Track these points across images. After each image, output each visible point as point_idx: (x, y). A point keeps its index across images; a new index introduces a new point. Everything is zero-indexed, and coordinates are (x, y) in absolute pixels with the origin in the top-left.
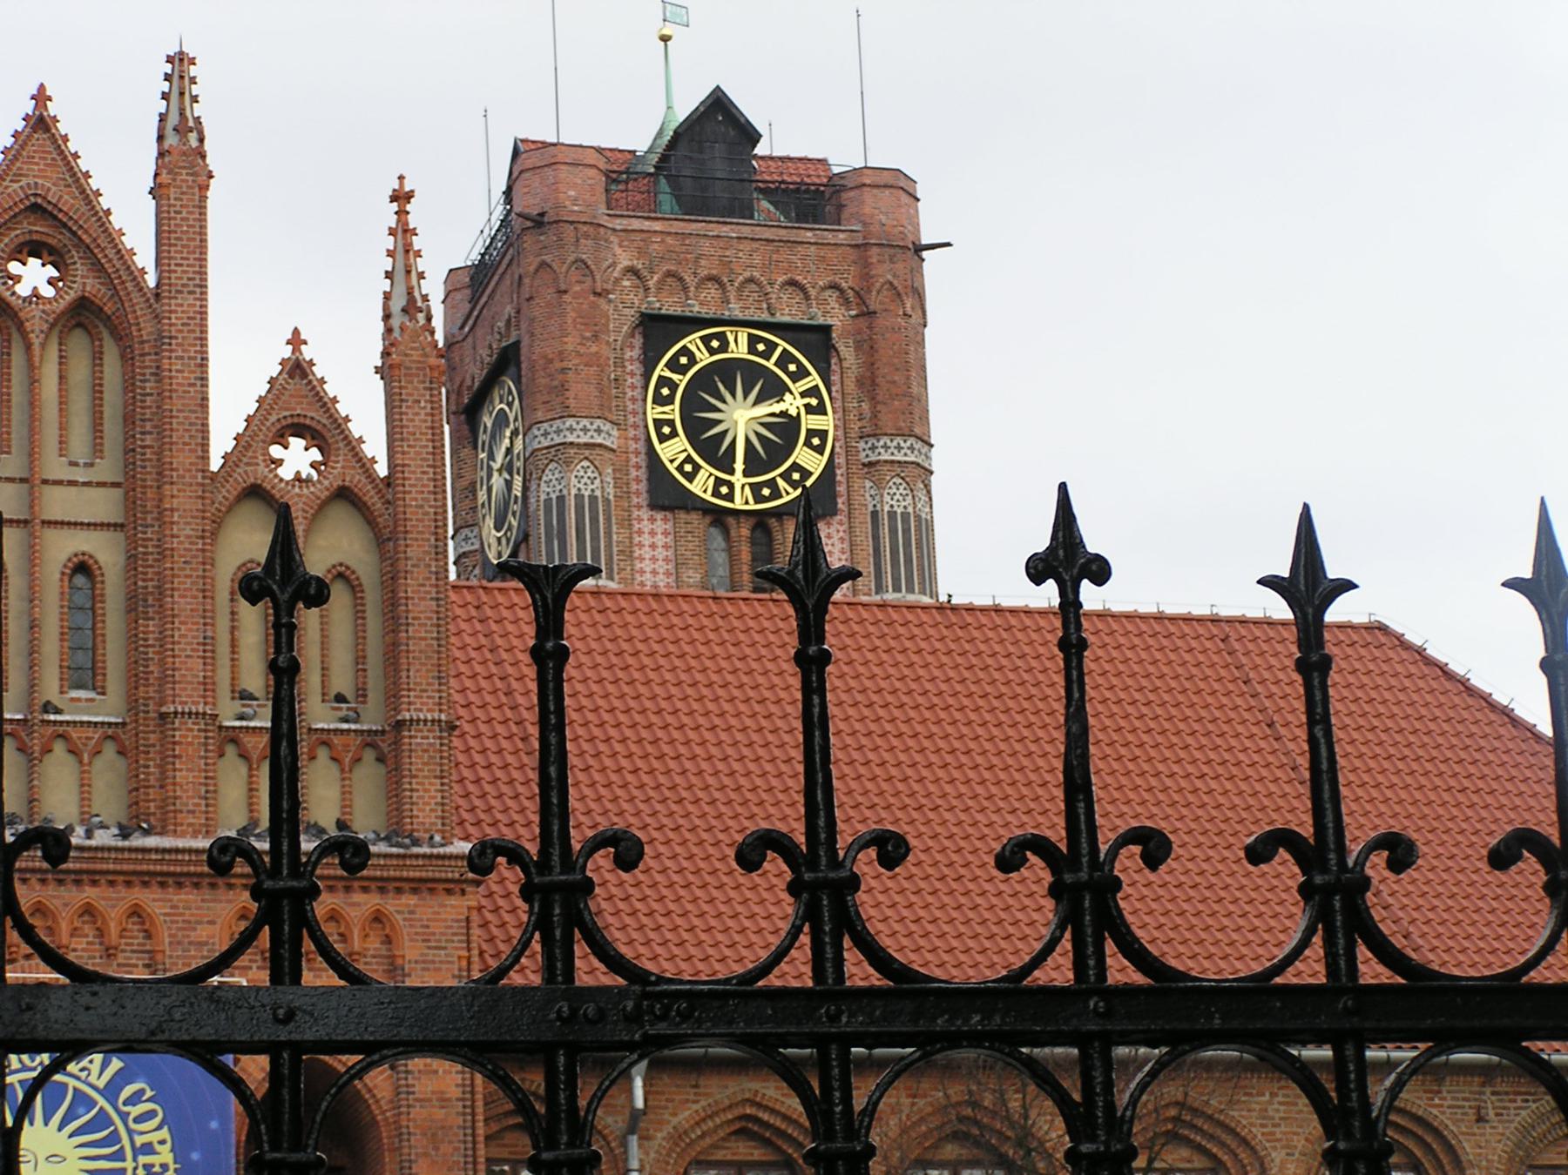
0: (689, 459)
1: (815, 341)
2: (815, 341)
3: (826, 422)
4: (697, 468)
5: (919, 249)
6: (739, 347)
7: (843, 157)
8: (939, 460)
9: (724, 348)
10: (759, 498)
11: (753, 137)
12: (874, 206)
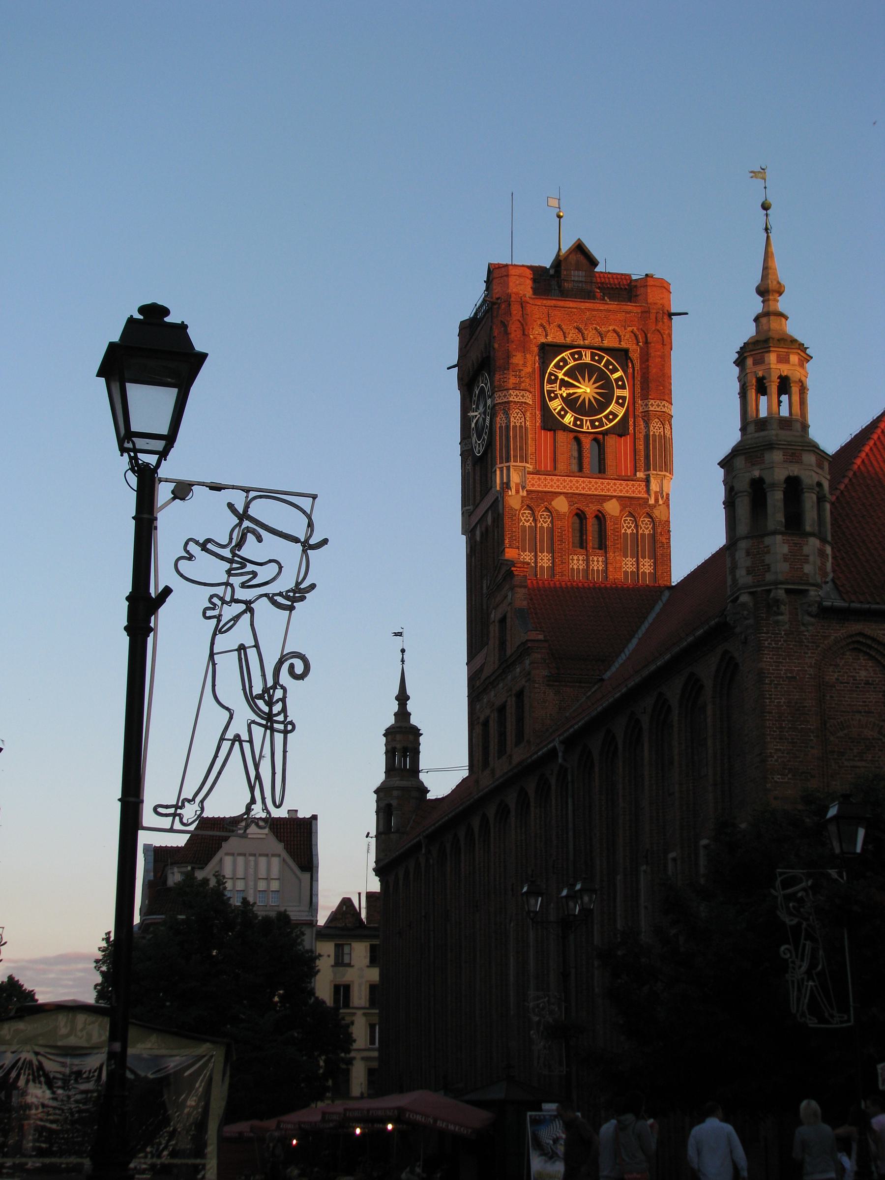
0: (563, 409)
1: (621, 355)
2: (621, 355)
3: (626, 393)
4: (566, 413)
5: (670, 315)
6: (587, 359)
7: (637, 273)
8: (674, 410)
9: (580, 358)
10: (594, 427)
11: (594, 263)
12: (653, 296)
